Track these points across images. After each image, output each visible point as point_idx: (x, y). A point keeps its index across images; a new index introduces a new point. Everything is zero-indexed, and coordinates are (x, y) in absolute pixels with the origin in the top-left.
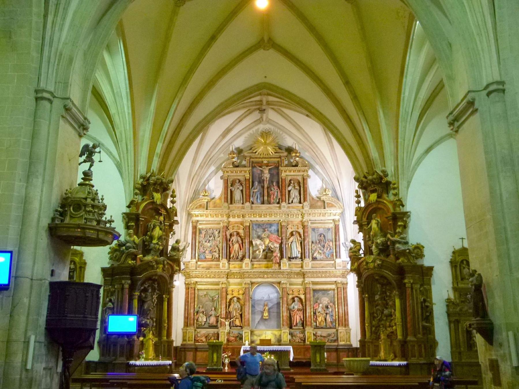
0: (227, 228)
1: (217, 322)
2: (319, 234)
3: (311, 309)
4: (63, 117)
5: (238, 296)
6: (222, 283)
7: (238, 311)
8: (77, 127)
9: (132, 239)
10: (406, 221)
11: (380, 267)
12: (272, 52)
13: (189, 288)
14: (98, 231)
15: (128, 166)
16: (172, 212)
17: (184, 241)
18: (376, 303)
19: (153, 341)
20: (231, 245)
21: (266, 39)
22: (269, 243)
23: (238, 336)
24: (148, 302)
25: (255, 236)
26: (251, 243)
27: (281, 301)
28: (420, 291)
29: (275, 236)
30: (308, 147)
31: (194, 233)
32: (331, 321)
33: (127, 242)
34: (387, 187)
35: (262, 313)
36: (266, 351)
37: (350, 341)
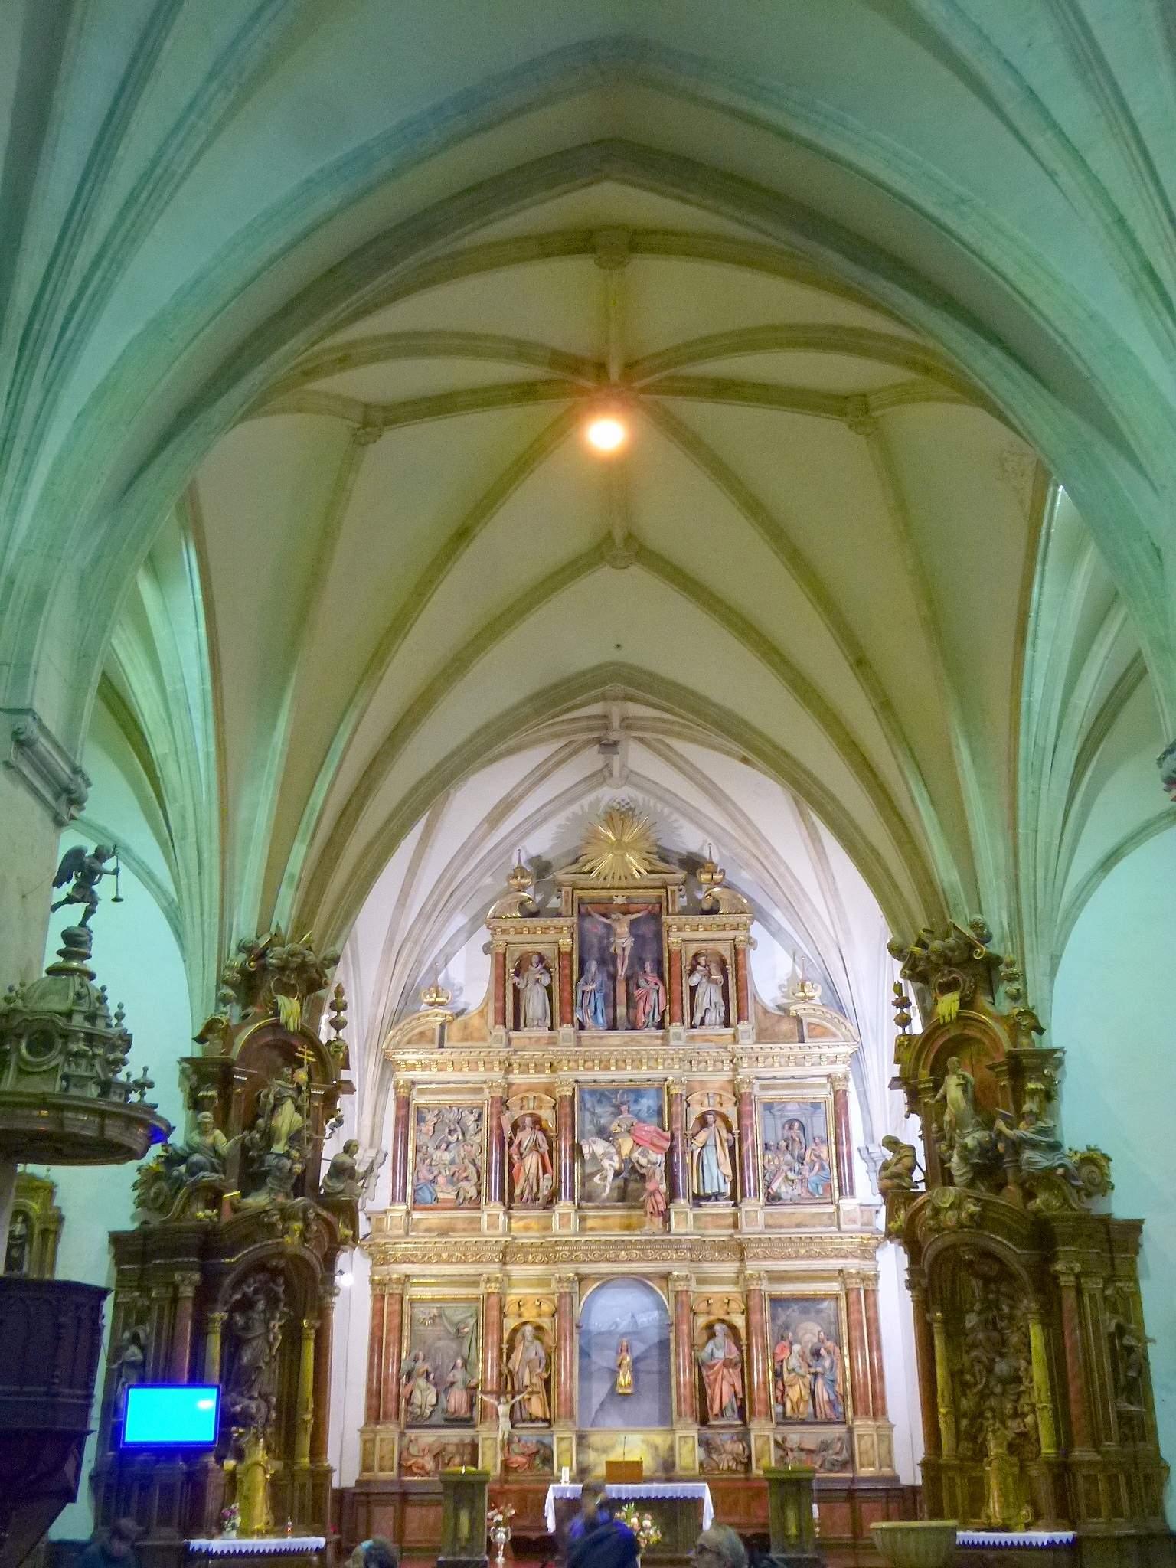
0: (503, 1103)
1: (472, 1405)
2: (784, 1120)
3: (765, 1359)
4: (8, 765)
5: (538, 1320)
6: (489, 1280)
7: (539, 1371)
8: (49, 797)
9: (209, 1140)
10: (1050, 1080)
11: (978, 1222)
12: (636, 572)
13: (383, 1297)
14: (103, 1114)
15: (202, 914)
16: (333, 1056)
17: (371, 1145)
18: (970, 1339)
19: (265, 1472)
20: (515, 1157)
21: (618, 535)
22: (632, 1151)
23: (537, 1453)
24: (254, 1343)
25: (589, 1127)
26: (577, 1151)
27: (672, 1336)
28: (1105, 1298)
29: (652, 1128)
30: (747, 855)
31: (402, 1121)
32: (830, 1401)
33: (193, 1150)
34: (989, 970)
35: (614, 1373)
36: (627, 1501)
37: (890, 1466)
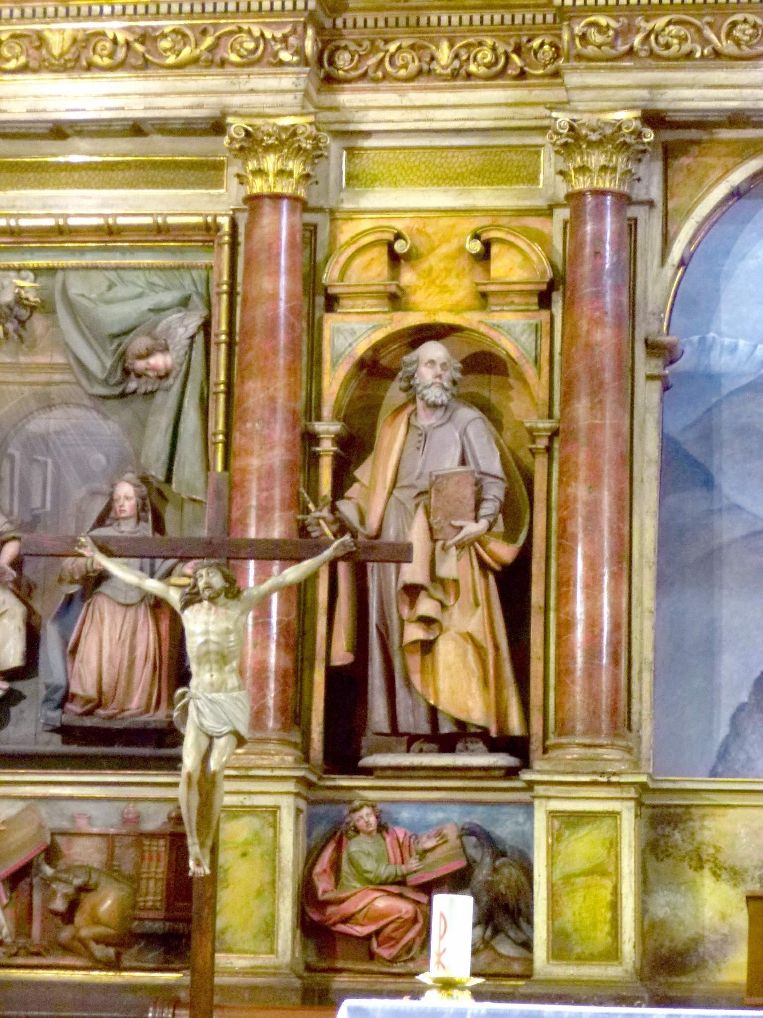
5: (469, 319)
7: (472, 528)
